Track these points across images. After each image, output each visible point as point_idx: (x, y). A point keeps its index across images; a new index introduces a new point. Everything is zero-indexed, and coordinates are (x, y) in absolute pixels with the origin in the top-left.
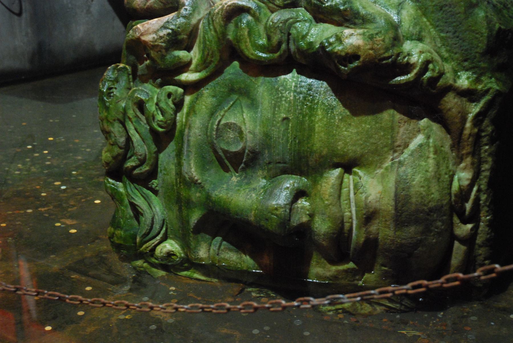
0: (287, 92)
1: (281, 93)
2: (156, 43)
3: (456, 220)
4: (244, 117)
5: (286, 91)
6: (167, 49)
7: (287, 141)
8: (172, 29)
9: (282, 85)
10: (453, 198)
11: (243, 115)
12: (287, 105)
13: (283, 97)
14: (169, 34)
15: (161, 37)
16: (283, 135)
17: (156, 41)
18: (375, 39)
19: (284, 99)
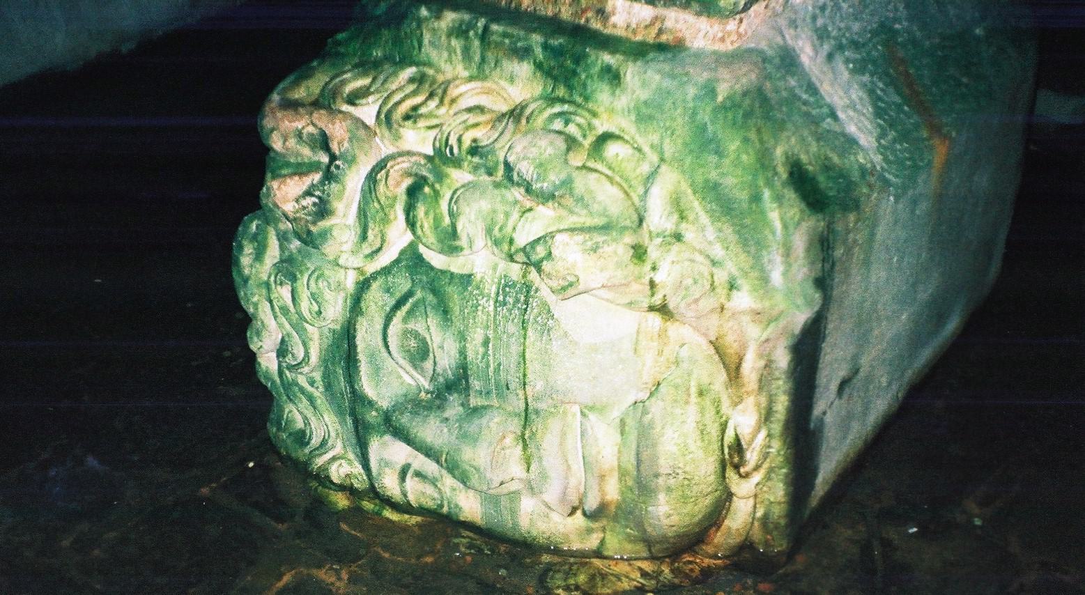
0: (485, 299)
1: (477, 299)
2: (298, 215)
3: (731, 473)
4: (429, 323)
5: (483, 298)
6: (314, 223)
7: (488, 366)
8: (319, 198)
9: (478, 288)
10: (726, 451)
11: (427, 322)
12: (485, 318)
13: (479, 305)
14: (314, 204)
15: (304, 208)
16: (483, 358)
17: (297, 212)
18: (601, 250)
19: (480, 308)
